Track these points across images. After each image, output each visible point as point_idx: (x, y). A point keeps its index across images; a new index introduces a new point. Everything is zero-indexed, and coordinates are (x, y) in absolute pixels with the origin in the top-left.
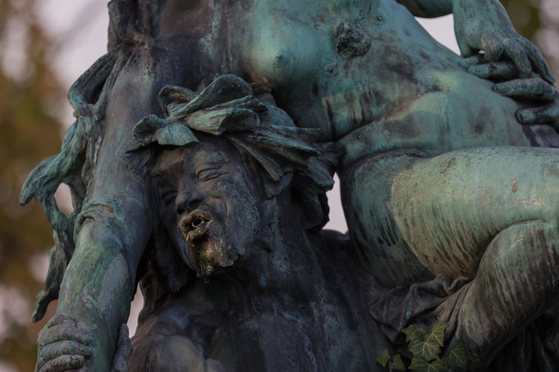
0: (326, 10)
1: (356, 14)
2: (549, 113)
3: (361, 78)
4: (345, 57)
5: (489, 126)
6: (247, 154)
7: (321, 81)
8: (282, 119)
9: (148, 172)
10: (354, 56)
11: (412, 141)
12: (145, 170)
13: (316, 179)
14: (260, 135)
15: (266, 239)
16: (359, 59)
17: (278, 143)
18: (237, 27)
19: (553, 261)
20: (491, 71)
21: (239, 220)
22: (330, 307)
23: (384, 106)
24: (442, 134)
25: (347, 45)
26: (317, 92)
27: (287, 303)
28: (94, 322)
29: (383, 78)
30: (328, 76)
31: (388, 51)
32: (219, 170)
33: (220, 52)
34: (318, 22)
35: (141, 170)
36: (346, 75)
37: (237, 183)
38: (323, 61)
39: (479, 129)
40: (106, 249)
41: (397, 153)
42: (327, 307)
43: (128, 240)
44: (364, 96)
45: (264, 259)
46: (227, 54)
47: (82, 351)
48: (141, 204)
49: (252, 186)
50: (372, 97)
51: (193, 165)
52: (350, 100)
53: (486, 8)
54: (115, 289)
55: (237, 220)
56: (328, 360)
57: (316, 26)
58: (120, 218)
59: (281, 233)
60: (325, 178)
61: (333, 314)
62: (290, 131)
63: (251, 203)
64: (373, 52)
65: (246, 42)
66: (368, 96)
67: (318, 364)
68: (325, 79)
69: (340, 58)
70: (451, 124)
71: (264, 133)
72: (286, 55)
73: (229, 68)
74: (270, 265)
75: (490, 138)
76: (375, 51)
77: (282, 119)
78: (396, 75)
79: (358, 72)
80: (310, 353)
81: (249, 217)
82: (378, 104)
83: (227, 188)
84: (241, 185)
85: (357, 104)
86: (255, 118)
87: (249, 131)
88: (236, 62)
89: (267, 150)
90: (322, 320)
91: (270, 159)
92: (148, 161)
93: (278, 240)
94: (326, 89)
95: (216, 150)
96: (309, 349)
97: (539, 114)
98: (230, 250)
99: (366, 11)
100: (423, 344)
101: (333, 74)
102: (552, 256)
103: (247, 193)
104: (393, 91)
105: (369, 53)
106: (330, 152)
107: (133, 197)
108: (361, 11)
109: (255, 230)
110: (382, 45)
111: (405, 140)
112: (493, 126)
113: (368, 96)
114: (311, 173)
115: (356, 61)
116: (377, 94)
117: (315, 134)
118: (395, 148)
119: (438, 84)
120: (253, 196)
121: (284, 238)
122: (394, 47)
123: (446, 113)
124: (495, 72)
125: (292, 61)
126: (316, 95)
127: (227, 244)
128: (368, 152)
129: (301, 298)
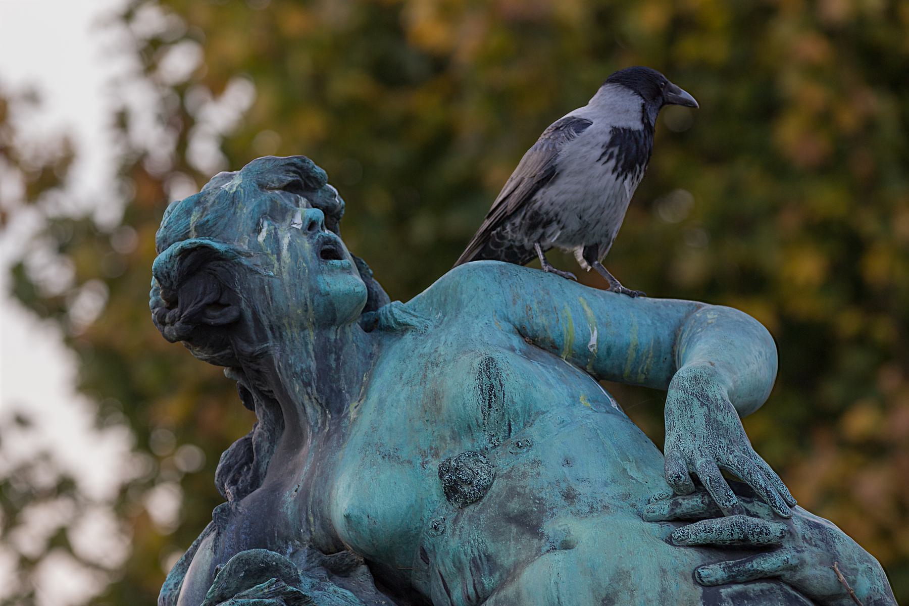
0: (443, 438)
1: (483, 440)
2: (755, 566)
3: (469, 536)
4: (456, 505)
10: (465, 505)
16: (472, 507)
18: (322, 472)
20: (672, 510)
23: (498, 574)
25: (456, 489)
30: (434, 536)
31: (512, 492)
33: (300, 510)
34: (430, 458)
36: (453, 534)
38: (427, 514)
44: (474, 560)
46: (307, 513)
50: (484, 562)
53: (689, 415)
57: (423, 465)
64: (491, 496)
65: (327, 494)
69: (451, 507)
70: (562, 599)
72: (356, 512)
73: (311, 532)
78: (514, 529)
79: (466, 527)
82: (491, 573)
85: (468, 574)
88: (318, 523)
94: (434, 552)
101: (439, 533)
105: (484, 500)
112: (632, 596)
115: (468, 511)
116: (489, 558)
119: (568, 538)
122: (522, 487)
123: (556, 583)
124: (678, 511)
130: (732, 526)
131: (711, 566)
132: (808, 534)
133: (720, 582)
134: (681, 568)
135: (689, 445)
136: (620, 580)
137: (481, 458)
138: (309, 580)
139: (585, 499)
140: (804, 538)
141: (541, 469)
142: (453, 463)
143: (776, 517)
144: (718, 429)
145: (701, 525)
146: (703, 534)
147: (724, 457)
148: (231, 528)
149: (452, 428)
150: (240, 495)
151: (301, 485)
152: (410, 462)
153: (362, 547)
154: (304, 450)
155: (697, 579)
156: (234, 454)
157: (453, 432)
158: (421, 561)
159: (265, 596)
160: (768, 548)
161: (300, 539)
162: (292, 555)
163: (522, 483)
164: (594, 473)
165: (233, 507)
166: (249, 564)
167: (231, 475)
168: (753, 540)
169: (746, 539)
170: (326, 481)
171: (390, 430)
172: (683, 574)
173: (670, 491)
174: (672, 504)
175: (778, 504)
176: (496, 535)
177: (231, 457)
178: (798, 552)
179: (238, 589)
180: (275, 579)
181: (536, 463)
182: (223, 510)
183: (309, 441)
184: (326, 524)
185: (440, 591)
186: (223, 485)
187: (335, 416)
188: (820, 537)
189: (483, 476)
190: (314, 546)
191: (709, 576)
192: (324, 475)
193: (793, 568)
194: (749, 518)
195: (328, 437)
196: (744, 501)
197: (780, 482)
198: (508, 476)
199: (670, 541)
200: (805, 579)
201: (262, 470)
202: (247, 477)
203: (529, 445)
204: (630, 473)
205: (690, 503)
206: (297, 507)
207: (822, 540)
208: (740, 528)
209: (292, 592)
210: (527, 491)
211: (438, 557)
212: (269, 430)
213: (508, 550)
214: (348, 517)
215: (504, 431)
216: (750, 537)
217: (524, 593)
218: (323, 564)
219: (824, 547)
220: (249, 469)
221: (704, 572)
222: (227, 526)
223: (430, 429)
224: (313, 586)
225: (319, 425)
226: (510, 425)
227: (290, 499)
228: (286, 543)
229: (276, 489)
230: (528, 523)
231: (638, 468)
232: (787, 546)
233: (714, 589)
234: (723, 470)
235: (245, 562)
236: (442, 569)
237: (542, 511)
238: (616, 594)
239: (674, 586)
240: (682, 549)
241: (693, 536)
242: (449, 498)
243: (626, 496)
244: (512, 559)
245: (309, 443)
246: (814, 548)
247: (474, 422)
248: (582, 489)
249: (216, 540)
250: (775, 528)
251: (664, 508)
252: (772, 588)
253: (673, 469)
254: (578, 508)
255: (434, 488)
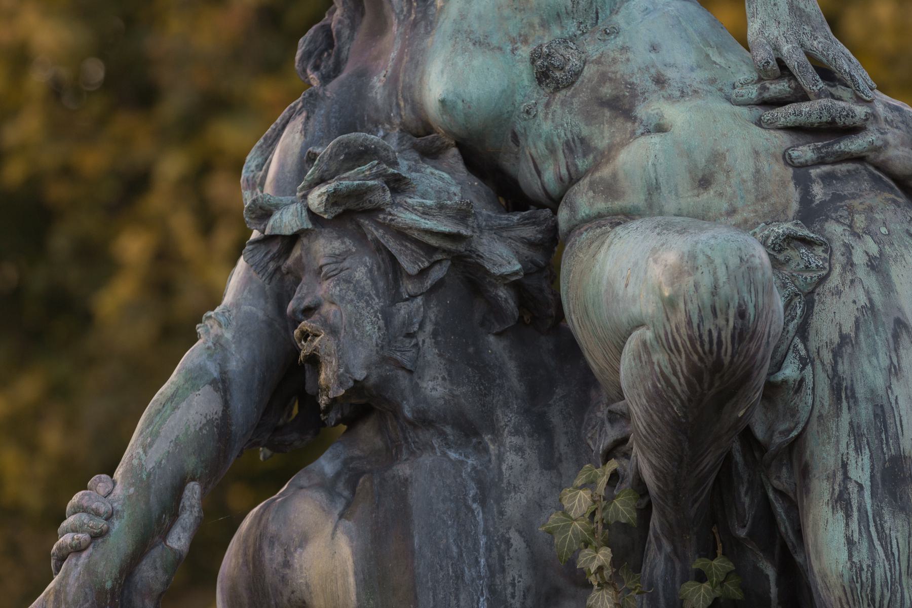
0: (531, 25)
1: (572, 28)
2: (843, 147)
4: (547, 90)
5: (721, 177)
6: (376, 241)
7: (518, 126)
8: (432, 188)
9: (278, 269)
10: (557, 89)
11: (617, 204)
12: (272, 266)
13: (488, 266)
14: (390, 214)
15: (398, 355)
16: (564, 92)
17: (407, 224)
18: (412, 59)
19: (663, 383)
20: (760, 94)
21: (356, 332)
22: (516, 440)
23: (591, 156)
24: (649, 194)
25: (548, 74)
26: (518, 142)
27: (451, 437)
28: (133, 485)
29: (589, 118)
30: (525, 120)
31: (604, 78)
32: (342, 265)
33: (390, 95)
34: (519, 44)
35: (266, 267)
36: (546, 118)
37: (358, 282)
38: (518, 98)
39: (704, 182)
40: (186, 381)
41: (603, 222)
42: (510, 440)
43: (234, 365)
44: (567, 143)
45: (404, 381)
46: (397, 98)
47: (92, 527)
48: (261, 314)
49: (381, 284)
50: (578, 145)
51: (315, 259)
52: (552, 151)
54: (177, 436)
55: (353, 333)
56: (501, 513)
57: (513, 51)
58: (228, 335)
59: (437, 343)
60: (505, 262)
61: (519, 450)
62: (427, 206)
63: (372, 308)
64: (583, 81)
65: (417, 79)
66: (572, 144)
67: (486, 520)
68: (523, 123)
69: (542, 92)
70: (661, 180)
71: (394, 212)
72: (451, 97)
73: (401, 116)
74: (416, 388)
75: (721, 195)
76: (586, 81)
77: (432, 188)
78: (607, 113)
79: (559, 111)
80: (475, 506)
81: (368, 328)
82: (585, 155)
83: (341, 290)
84: (362, 284)
86: (384, 191)
87: (379, 209)
88: (408, 107)
89: (401, 234)
90: (500, 458)
91: (409, 245)
92: (274, 254)
93: (430, 352)
94: (526, 136)
95: (339, 238)
96: (474, 500)
97: (824, 151)
98: (342, 374)
99: (589, 23)
100: (577, 494)
101: (531, 117)
102: (659, 375)
103: (369, 295)
104: (602, 134)
105: (577, 84)
106: (524, 225)
107: (250, 305)
108: (581, 23)
109: (377, 345)
110: (598, 71)
111: (609, 204)
113: (572, 144)
114: (482, 257)
115: (560, 95)
116: (582, 140)
117: (463, 208)
118: (600, 216)
119: (661, 122)
120: (379, 299)
121: (439, 351)
122: (613, 73)
123: (654, 165)
124: (766, 95)
125: (460, 105)
126: (518, 146)
127: (339, 366)
128: (575, 222)
129: (470, 429)
130: (821, 109)
131: (800, 148)
132: (890, 116)
133: (809, 163)
134: (772, 150)
135: (774, 31)
136: (716, 161)
137: (571, 45)
138: (406, 162)
139: (675, 84)
140: (886, 120)
141: (630, 55)
142: (545, 50)
143: (860, 100)
144: (801, 16)
145: (790, 108)
146: (793, 118)
147: (808, 43)
148: (320, 112)
149: (541, 16)
150: (326, 79)
151: (390, 70)
152: (500, 49)
153: (455, 130)
154: (388, 39)
155: (787, 160)
156: (313, 40)
157: (542, 19)
158: (511, 144)
159: (366, 178)
160: (853, 130)
161: (391, 123)
162: (384, 138)
163: (613, 69)
164: (679, 58)
165: (321, 92)
166: (349, 147)
167: (312, 61)
168: (840, 122)
169: (833, 121)
170: (416, 67)
171: (479, 17)
172: (774, 155)
173: (755, 76)
174: (760, 88)
175: (861, 88)
176: (589, 118)
177: (310, 42)
178: (882, 133)
179: (337, 172)
180: (376, 162)
181: (624, 49)
182: (311, 95)
183: (395, 28)
184: (417, 108)
185: (530, 172)
186: (304, 71)
187: (421, 4)
188: (900, 119)
189: (575, 61)
190: (405, 130)
191: (799, 157)
192: (415, 60)
193: (878, 150)
194: (836, 102)
195: (415, 24)
196: (829, 85)
197: (860, 67)
198: (598, 62)
199: (759, 123)
200: (889, 159)
201: (343, 55)
202: (328, 63)
203: (616, 32)
204: (714, 59)
205: (778, 88)
206: (386, 92)
207: (903, 122)
208: (828, 111)
209: (393, 174)
210: (618, 76)
211: (530, 140)
212: (349, 18)
213: (602, 133)
214: (443, 102)
215: (592, 18)
216: (837, 120)
217: (621, 175)
218: (415, 147)
219: (904, 129)
220: (329, 55)
221: (795, 154)
222: (316, 111)
223: (518, 16)
224: (410, 168)
225: (405, 13)
226: (597, 13)
227: (379, 85)
228: (376, 126)
229: (363, 75)
230: (620, 106)
231: (720, 53)
232: (871, 128)
233: (803, 170)
234: (809, 56)
235: (347, 145)
236: (533, 151)
237: (634, 96)
238: (712, 174)
239: (767, 168)
240: (772, 131)
241: (782, 120)
242: (540, 82)
243: (713, 81)
244: (606, 141)
245: (395, 29)
246: (896, 131)
247: (563, 10)
248: (670, 74)
249: (306, 123)
250: (860, 111)
251: (752, 92)
252: (857, 169)
253: (762, 54)
254: (669, 92)
255: (524, 74)
